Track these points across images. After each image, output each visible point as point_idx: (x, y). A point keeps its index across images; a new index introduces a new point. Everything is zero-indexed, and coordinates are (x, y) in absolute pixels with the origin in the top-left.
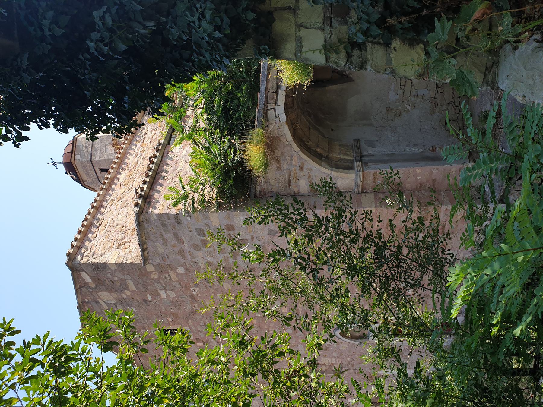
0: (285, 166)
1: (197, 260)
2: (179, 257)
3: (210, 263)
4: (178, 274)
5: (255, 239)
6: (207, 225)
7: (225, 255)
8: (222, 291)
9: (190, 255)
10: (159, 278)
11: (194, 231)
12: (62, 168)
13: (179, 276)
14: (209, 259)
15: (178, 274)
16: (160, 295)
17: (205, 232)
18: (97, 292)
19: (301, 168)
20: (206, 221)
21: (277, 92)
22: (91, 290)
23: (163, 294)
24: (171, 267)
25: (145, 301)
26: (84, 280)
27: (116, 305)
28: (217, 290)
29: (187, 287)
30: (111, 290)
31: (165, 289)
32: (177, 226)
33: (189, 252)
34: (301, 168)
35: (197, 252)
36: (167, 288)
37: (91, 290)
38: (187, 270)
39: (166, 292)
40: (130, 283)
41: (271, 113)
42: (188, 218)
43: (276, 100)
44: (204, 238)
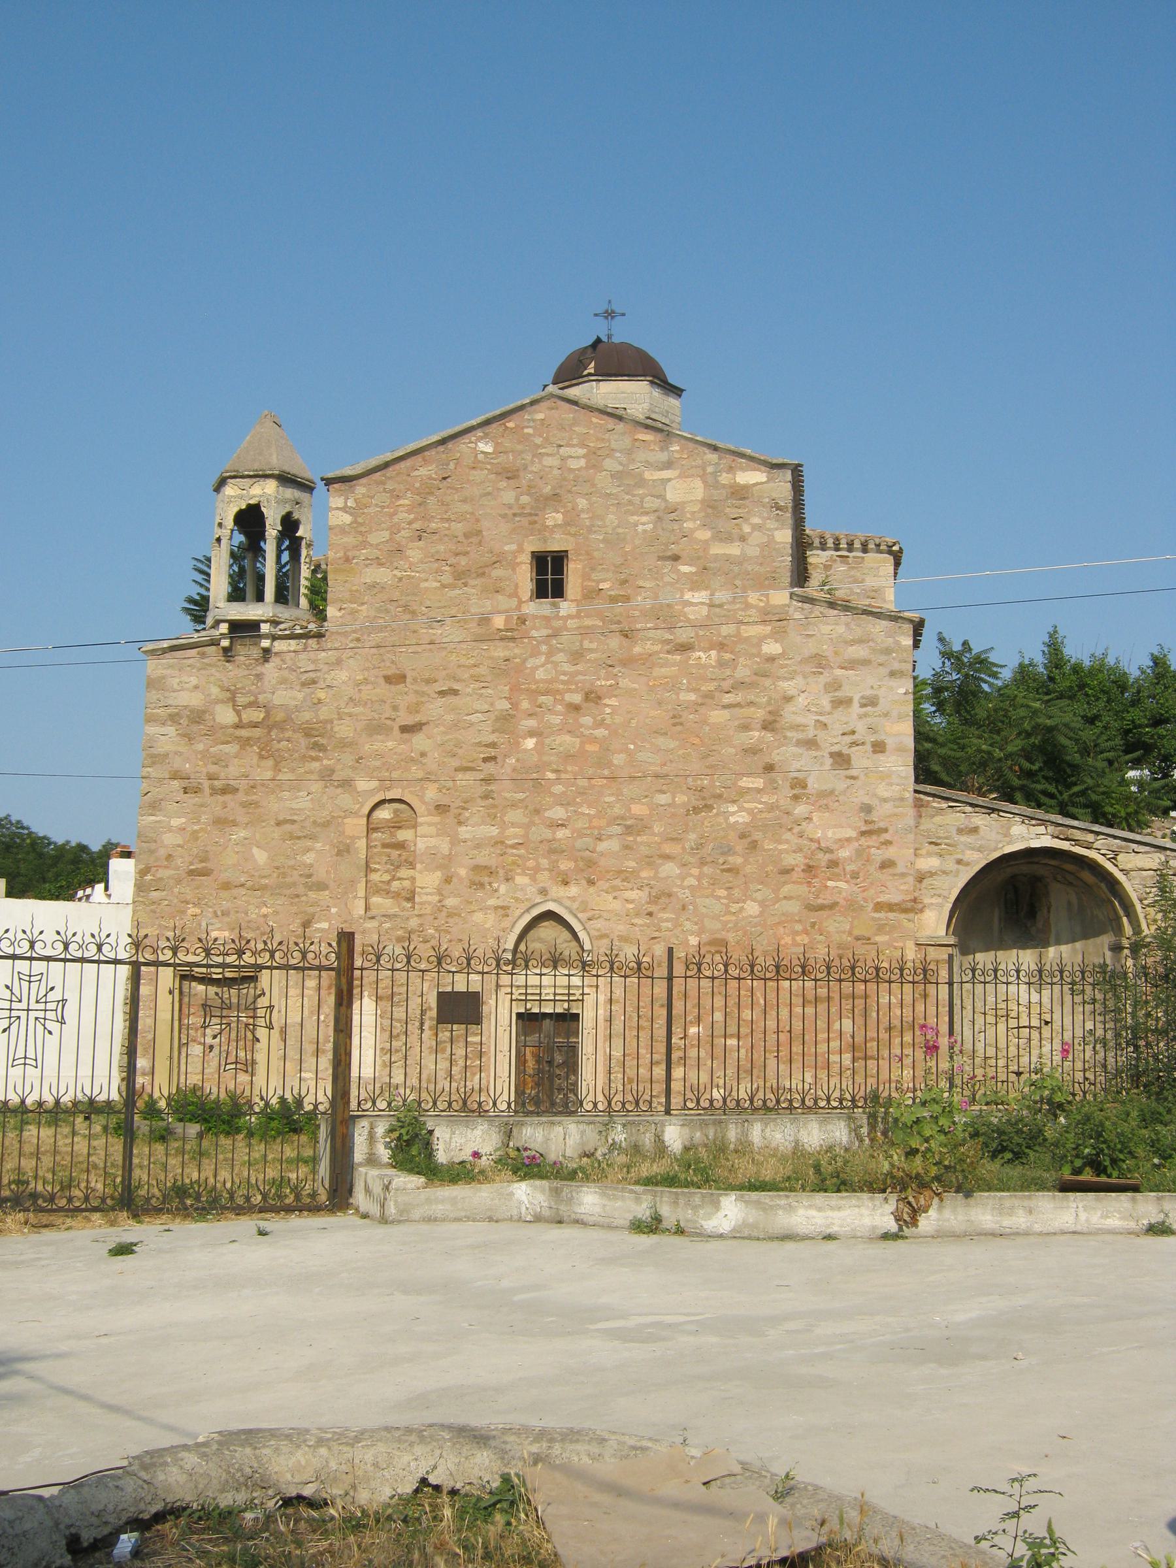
0: (964, 839)
1: (799, 681)
2: (806, 653)
3: (788, 699)
4: (762, 639)
5: (852, 782)
6: (886, 715)
7: (812, 728)
8: (702, 704)
9: (814, 673)
10: (748, 606)
11: (869, 692)
12: (600, 329)
13: (755, 641)
14: (802, 700)
15: (762, 639)
16: (691, 590)
17: (869, 708)
18: (703, 477)
19: (959, 862)
20: (894, 714)
21: (1067, 839)
22: (710, 469)
23: (701, 596)
24: (779, 635)
25: (676, 558)
26: (743, 470)
27: (662, 497)
28: (709, 695)
29: (721, 647)
30: (711, 507)
31: (711, 605)
32: (883, 671)
33: (821, 673)
34: (959, 862)
35: (821, 686)
36: (717, 610)
37: (710, 469)
38: (771, 659)
39: (702, 603)
40: (734, 550)
41: (1042, 829)
42: (902, 691)
43: (1057, 837)
44: (856, 704)
